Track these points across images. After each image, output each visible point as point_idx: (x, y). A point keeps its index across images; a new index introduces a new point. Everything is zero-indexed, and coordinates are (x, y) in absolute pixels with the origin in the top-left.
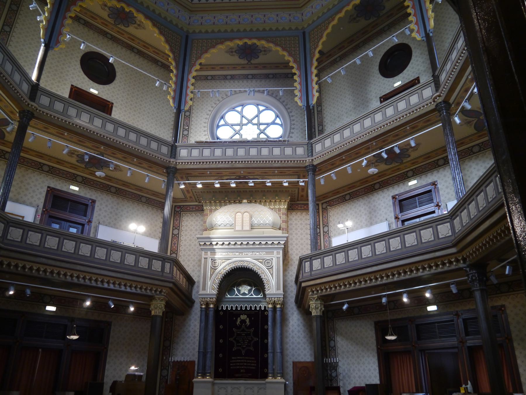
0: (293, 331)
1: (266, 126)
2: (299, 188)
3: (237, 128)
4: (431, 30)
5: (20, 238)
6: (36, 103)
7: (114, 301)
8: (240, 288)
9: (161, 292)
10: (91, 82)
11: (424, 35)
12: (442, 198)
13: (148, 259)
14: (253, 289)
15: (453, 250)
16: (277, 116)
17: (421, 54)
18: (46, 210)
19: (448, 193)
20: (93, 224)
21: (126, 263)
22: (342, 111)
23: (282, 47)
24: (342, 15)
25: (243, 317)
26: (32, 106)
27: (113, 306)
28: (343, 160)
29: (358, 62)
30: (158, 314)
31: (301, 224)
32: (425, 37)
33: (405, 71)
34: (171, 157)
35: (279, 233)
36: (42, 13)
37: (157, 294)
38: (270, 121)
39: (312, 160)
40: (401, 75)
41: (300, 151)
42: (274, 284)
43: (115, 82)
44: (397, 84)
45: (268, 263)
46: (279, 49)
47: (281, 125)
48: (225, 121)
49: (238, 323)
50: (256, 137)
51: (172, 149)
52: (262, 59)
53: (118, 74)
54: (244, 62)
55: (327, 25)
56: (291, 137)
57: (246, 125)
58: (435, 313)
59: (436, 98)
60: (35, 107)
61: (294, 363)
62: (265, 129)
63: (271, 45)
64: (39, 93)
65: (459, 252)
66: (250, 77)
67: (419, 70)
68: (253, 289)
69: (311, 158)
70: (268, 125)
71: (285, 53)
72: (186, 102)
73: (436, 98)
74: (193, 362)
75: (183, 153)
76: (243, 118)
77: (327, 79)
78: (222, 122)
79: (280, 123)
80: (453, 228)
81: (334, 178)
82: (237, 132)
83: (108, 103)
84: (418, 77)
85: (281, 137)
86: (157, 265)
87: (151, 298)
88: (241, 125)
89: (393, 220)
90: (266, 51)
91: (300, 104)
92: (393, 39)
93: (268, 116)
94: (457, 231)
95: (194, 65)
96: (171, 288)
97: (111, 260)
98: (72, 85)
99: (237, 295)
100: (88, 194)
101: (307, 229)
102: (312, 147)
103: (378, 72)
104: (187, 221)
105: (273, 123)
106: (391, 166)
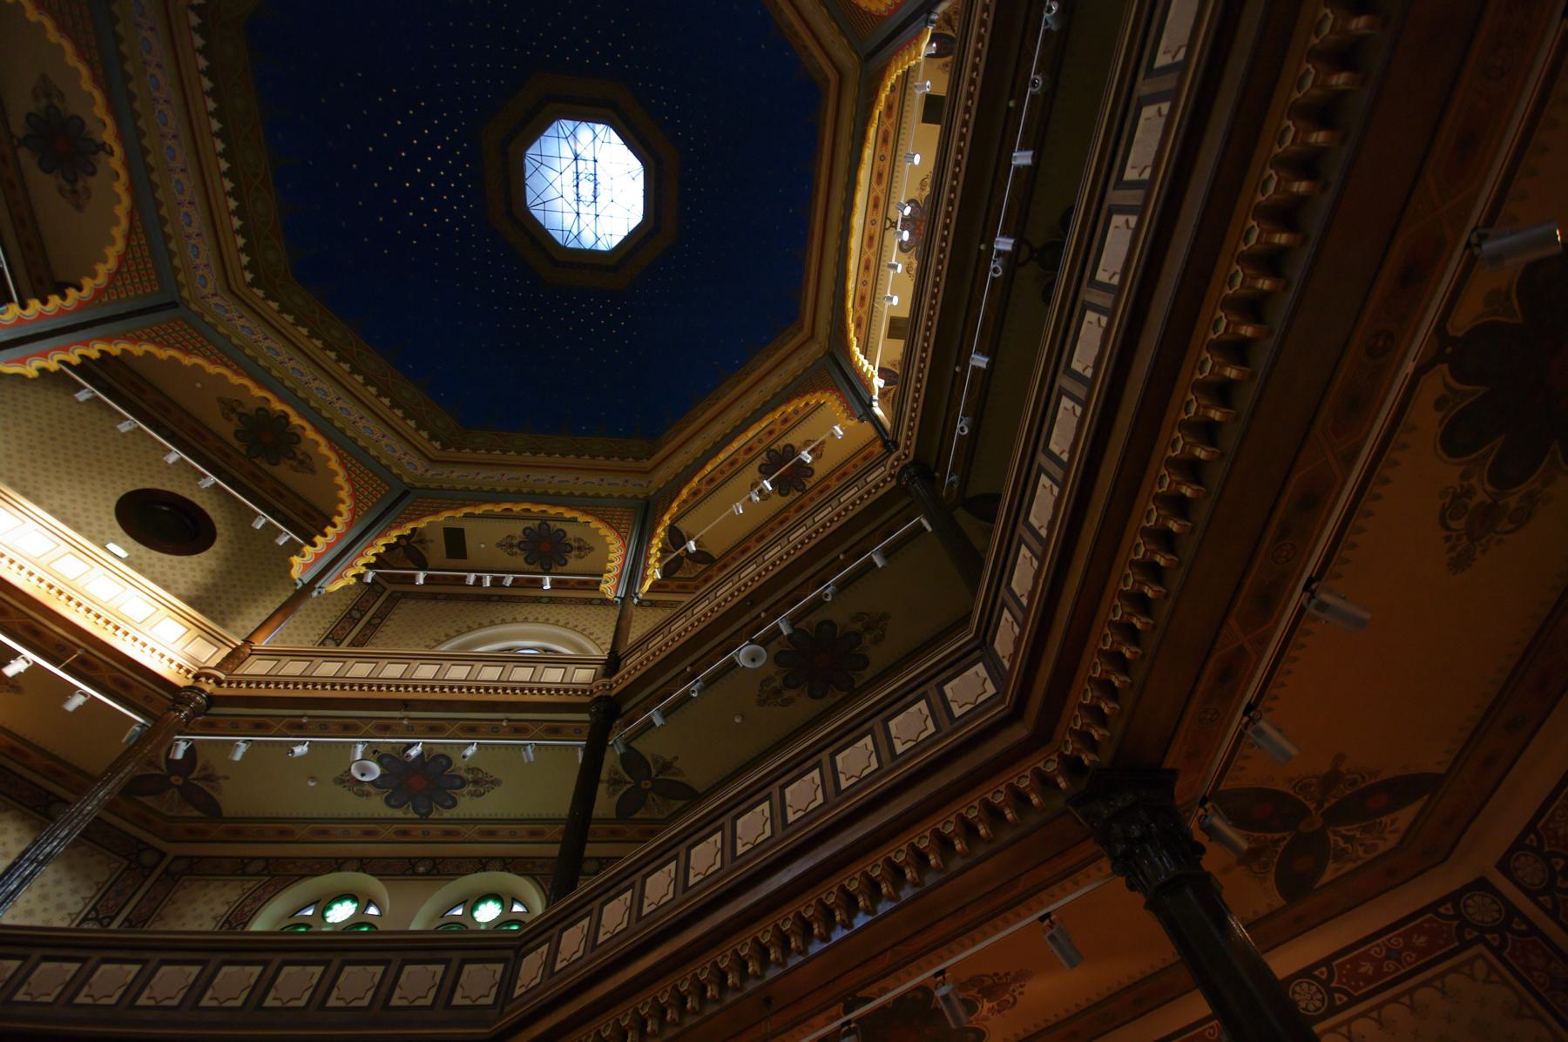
4: (323, 591)
11: (306, 580)
23: (126, 253)
32: (303, 584)
33: (155, 554)
40: (142, 548)
55: (219, 361)
59: (208, 676)
73: (208, 679)
92: (260, 519)
103: (122, 494)
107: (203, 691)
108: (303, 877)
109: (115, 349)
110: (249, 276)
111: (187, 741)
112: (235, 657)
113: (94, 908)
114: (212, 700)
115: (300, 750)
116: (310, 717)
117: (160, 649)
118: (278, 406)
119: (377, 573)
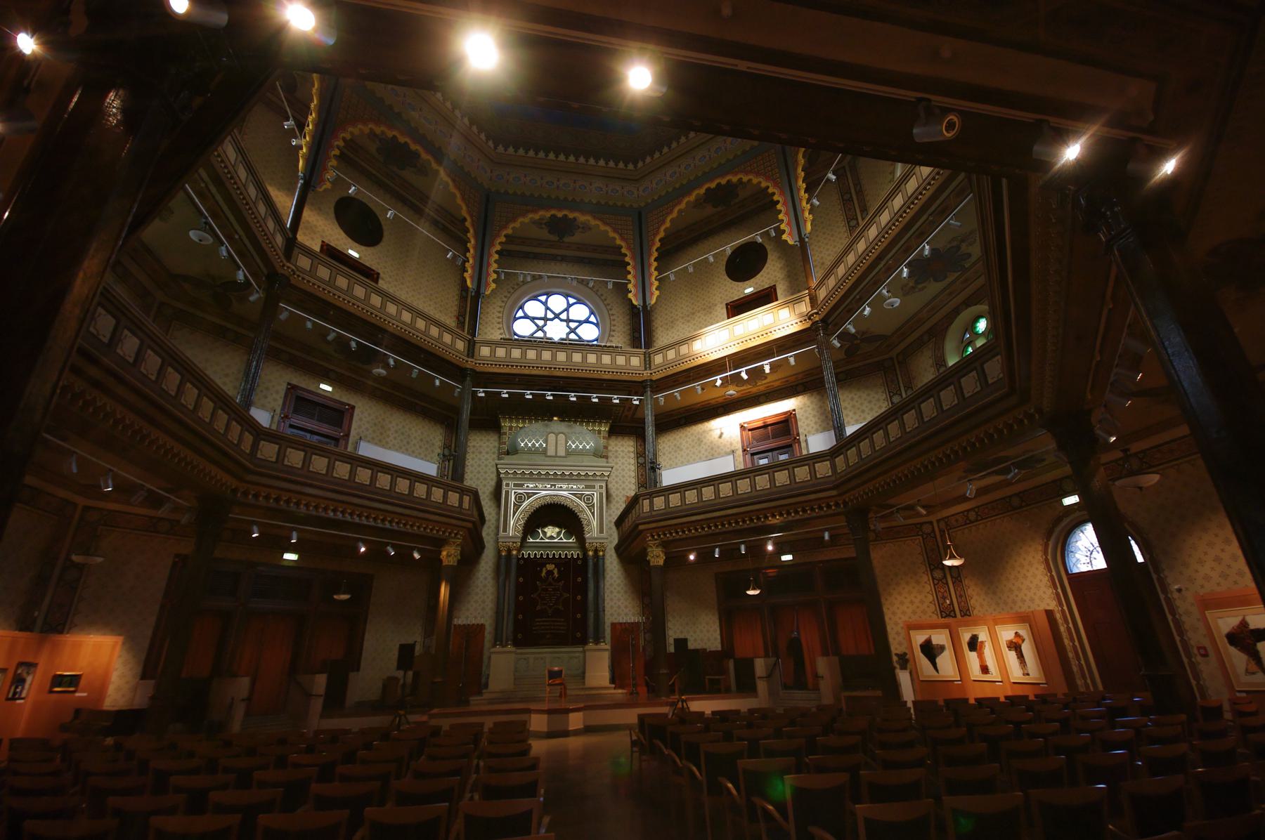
0: (611, 585)
1: (577, 324)
2: (625, 407)
3: (541, 323)
4: (808, 235)
5: (275, 456)
6: (292, 264)
7: (394, 546)
8: (546, 530)
9: (456, 534)
10: (350, 240)
11: (798, 239)
12: (801, 431)
13: (442, 491)
14: (563, 531)
15: (834, 493)
16: (592, 313)
17: (779, 258)
18: (286, 417)
19: (808, 425)
20: (351, 440)
21: (415, 495)
22: (677, 315)
24: (692, 198)
25: (550, 567)
26: (288, 267)
27: (393, 553)
28: (690, 376)
29: (711, 259)
30: (451, 564)
31: (623, 451)
33: (759, 276)
34: (468, 356)
35: (602, 462)
36: (298, 134)
37: (452, 538)
38: (583, 318)
39: (651, 374)
40: (752, 280)
41: (635, 361)
42: (595, 526)
43: (382, 244)
44: (749, 290)
45: (588, 500)
46: (607, 228)
47: (597, 325)
48: (524, 312)
49: (543, 574)
50: (564, 337)
51: (469, 344)
52: (577, 238)
53: (386, 234)
54: (555, 238)
56: (611, 341)
57: (552, 320)
58: (790, 563)
59: (812, 315)
60: (293, 270)
61: (613, 625)
62: (577, 328)
63: (598, 222)
64: (296, 250)
65: (839, 495)
66: (559, 258)
67: (775, 277)
68: (563, 531)
69: (649, 372)
70: (581, 323)
71: (617, 236)
72: (487, 285)
74: (482, 627)
75: (485, 351)
76: (548, 311)
77: (671, 274)
78: (520, 313)
79: (595, 322)
80: (833, 467)
81: (679, 398)
82: (540, 329)
83: (372, 272)
84: (775, 285)
85: (596, 340)
86: (453, 498)
87: (440, 543)
88: (545, 319)
89: (740, 452)
90: (586, 228)
91: (635, 302)
93: (579, 312)
94: (839, 471)
95: (498, 236)
96: (469, 529)
97: (397, 490)
98: (323, 242)
99: (542, 539)
100: (346, 398)
101: (629, 457)
102: (650, 357)
104: (475, 440)
105: (587, 321)
106: (742, 388)
107: (817, 321)
108: (947, 328)
109: (658, 244)
110: (631, 166)
111: (834, 339)
112: (813, 300)
113: (889, 392)
114: (823, 320)
115: (867, 311)
116: (858, 294)
117: (789, 324)
118: (702, 191)
119: (817, 196)
